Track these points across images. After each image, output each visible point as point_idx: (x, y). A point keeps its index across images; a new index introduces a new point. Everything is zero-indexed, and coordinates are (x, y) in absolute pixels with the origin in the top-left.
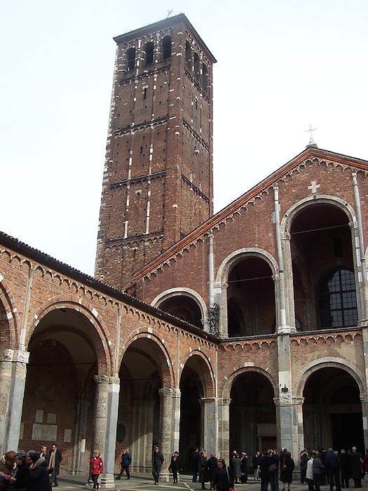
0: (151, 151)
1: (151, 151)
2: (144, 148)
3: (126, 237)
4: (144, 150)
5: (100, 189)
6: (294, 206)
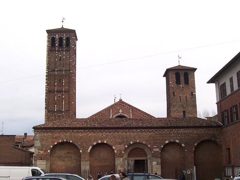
0: (64, 81)
1: (64, 82)
2: (61, 79)
3: (56, 110)
4: (61, 81)
5: (45, 92)
6: (115, 116)
